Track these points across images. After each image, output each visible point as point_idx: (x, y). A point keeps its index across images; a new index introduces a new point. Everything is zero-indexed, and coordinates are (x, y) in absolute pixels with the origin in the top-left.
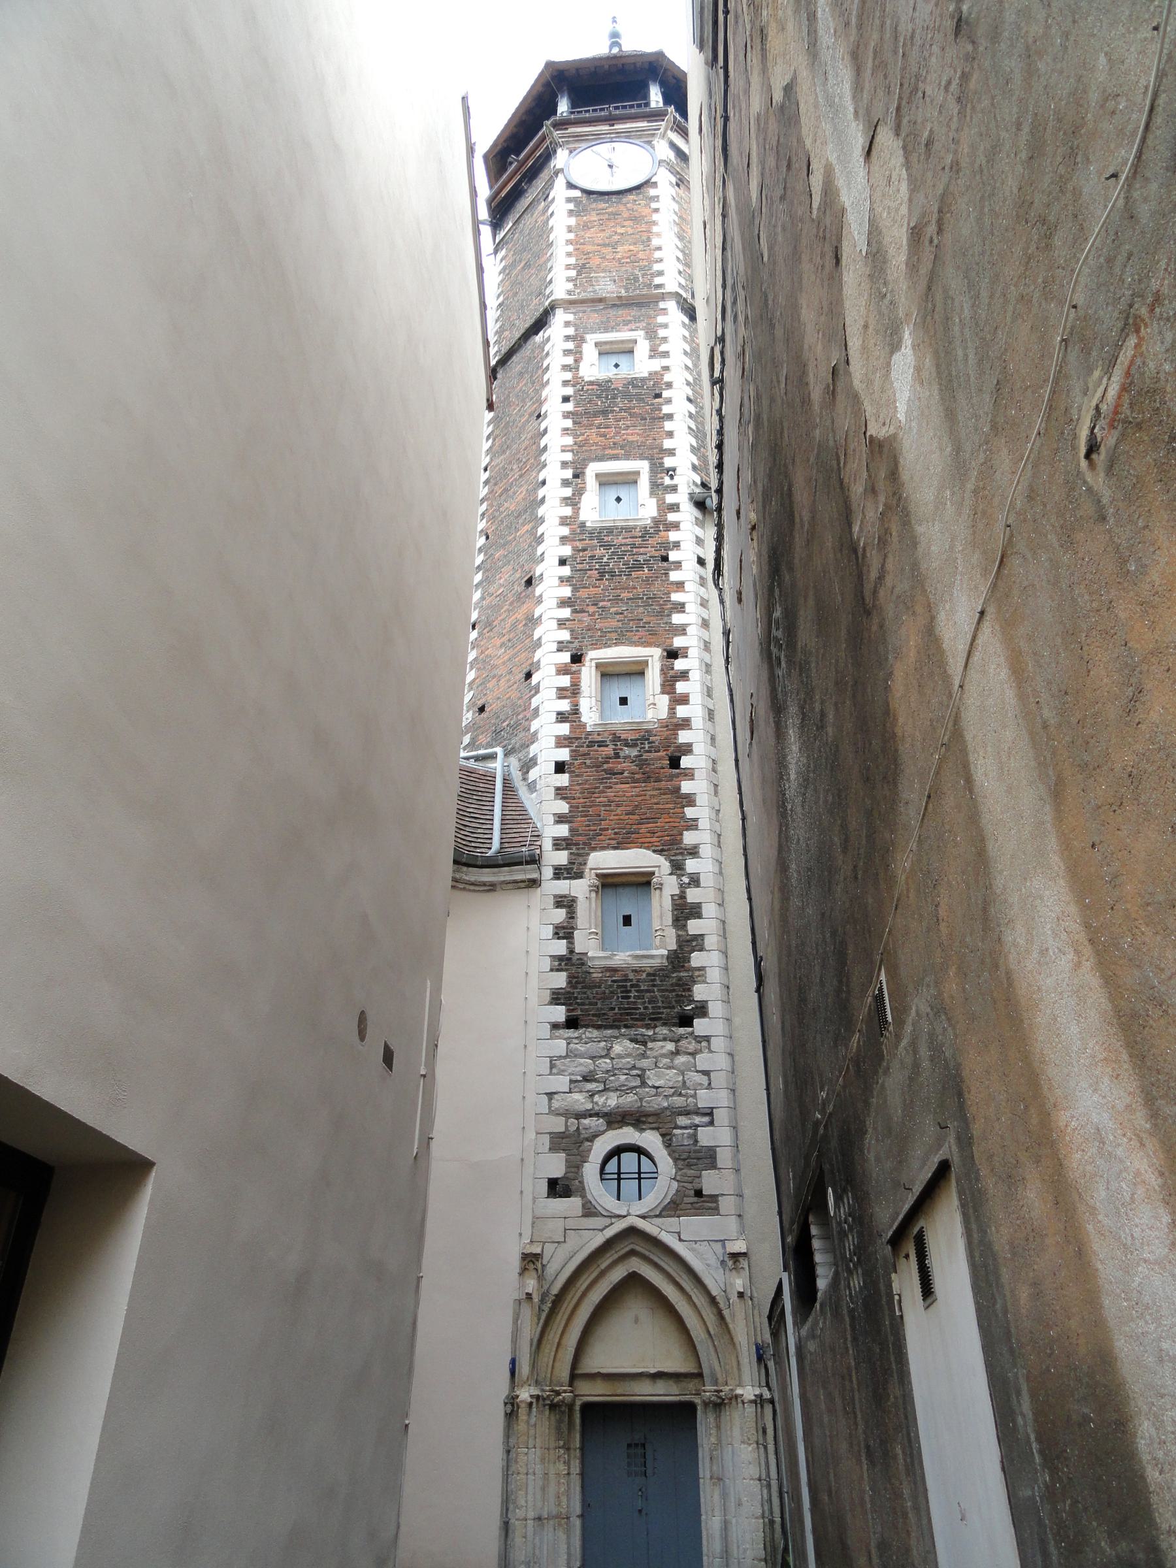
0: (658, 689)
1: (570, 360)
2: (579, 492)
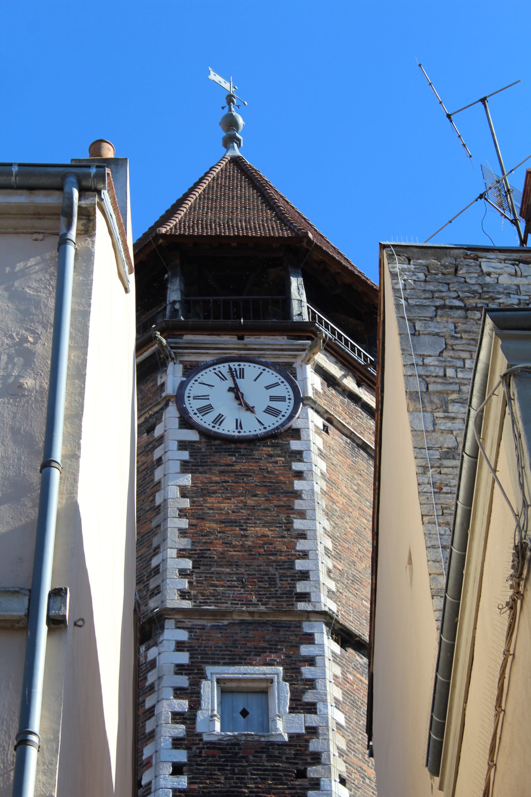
1: (183, 705)
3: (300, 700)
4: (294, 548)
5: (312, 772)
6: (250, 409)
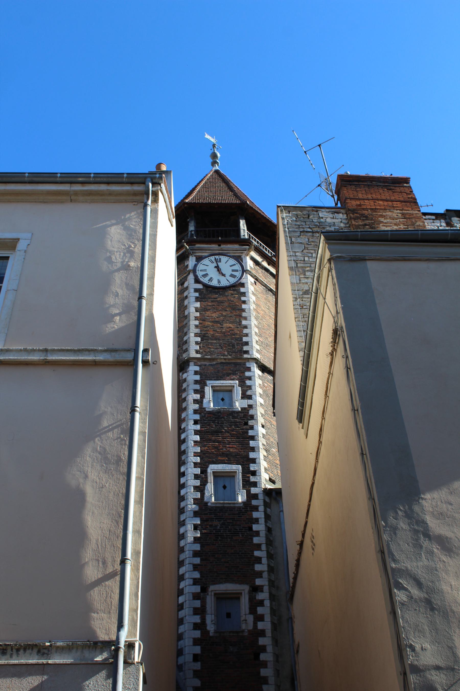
0: (248, 611)
1: (198, 396)
2: (204, 482)
3: (245, 394)
4: (242, 332)
5: (251, 423)
6: (224, 275)
